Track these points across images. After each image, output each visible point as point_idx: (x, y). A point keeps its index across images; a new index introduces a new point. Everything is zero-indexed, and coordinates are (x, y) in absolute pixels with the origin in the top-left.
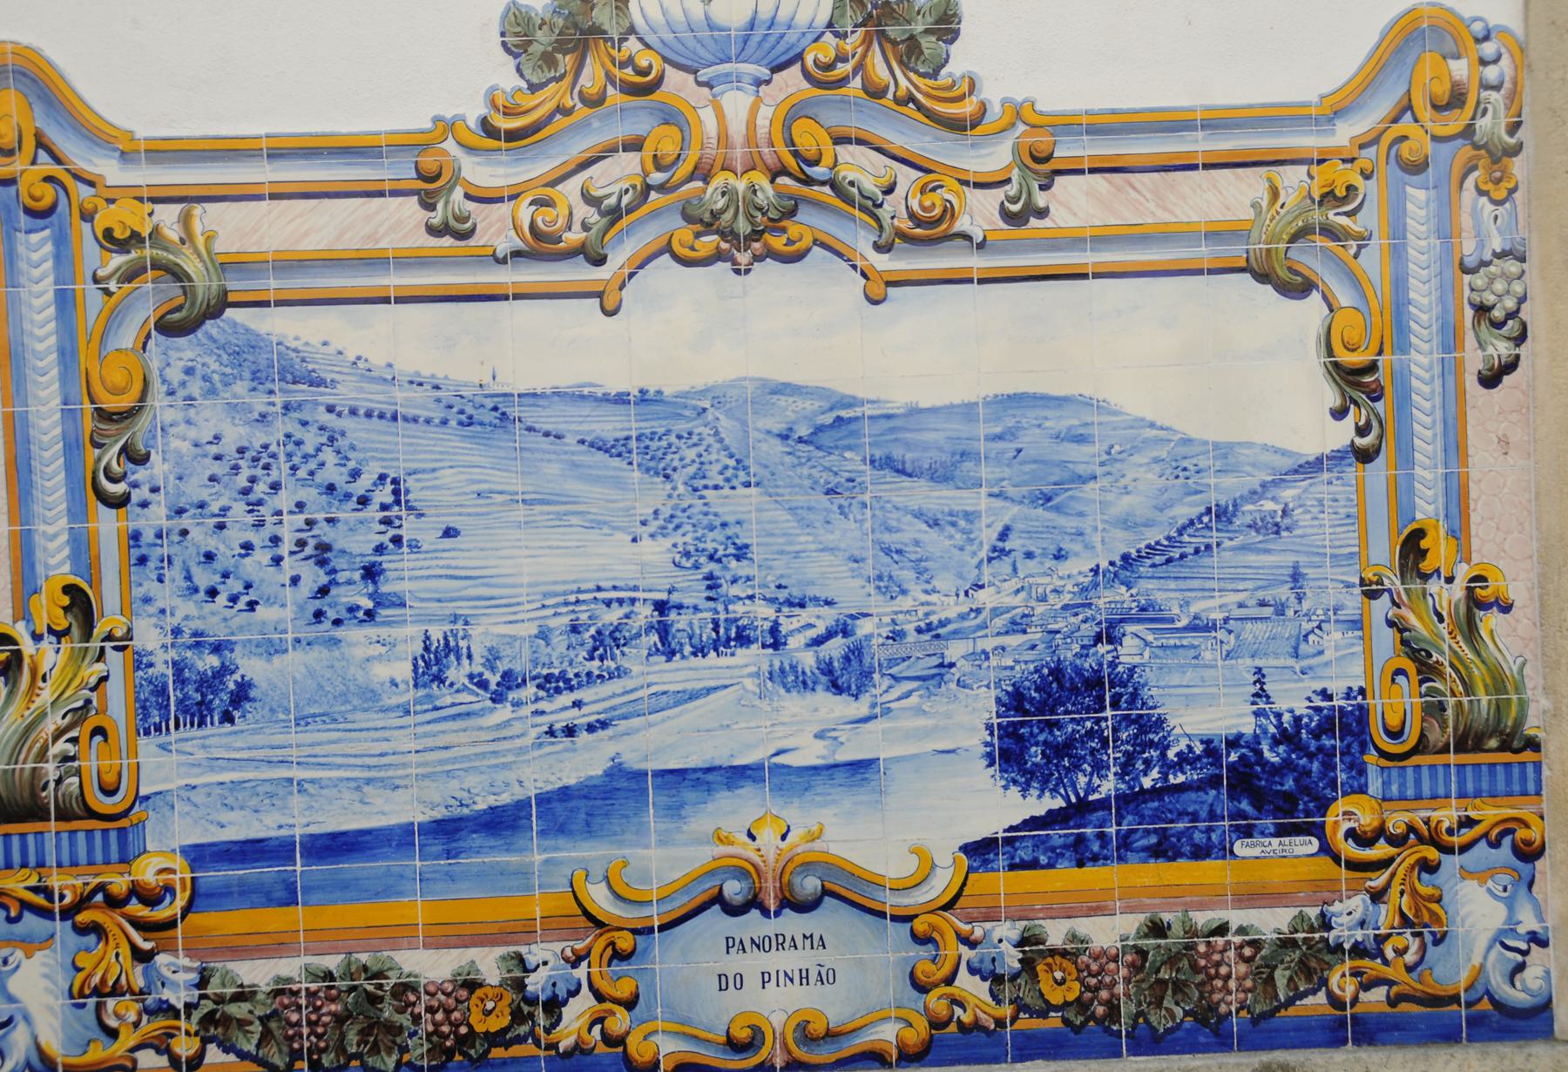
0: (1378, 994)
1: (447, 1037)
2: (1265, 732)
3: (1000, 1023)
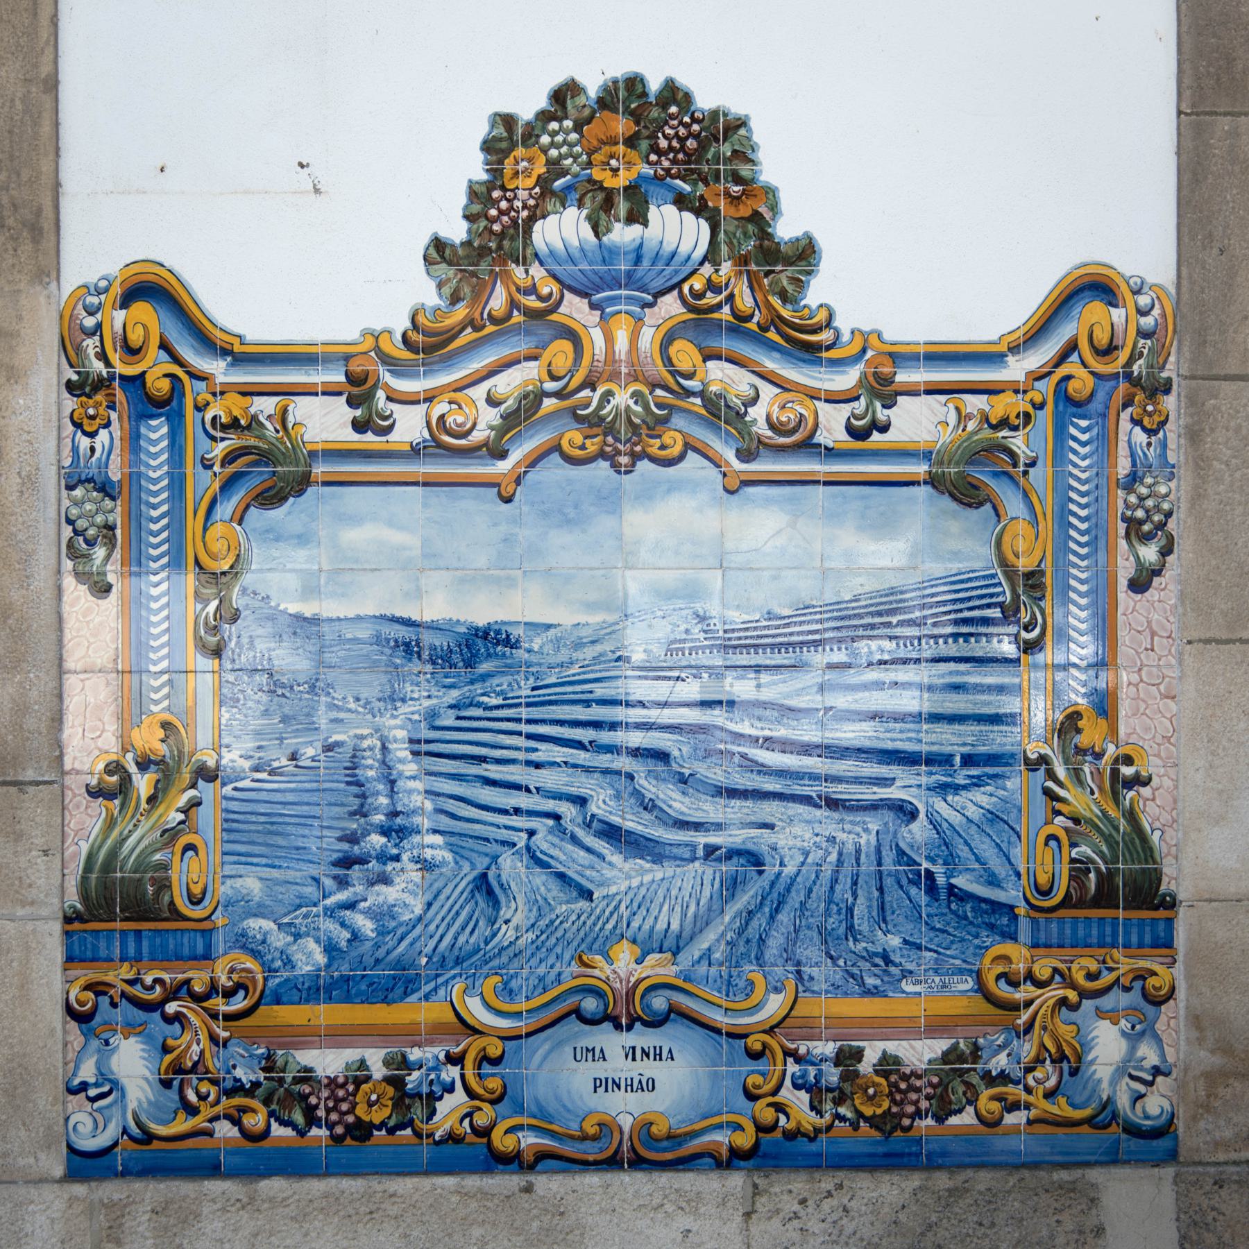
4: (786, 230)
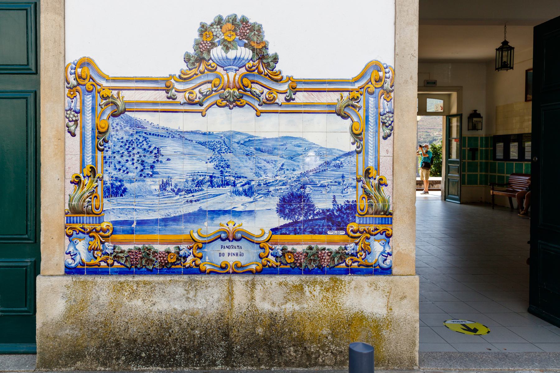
0: (356, 264)
1: (163, 263)
2: (335, 208)
3: (277, 266)
4: (271, 51)
